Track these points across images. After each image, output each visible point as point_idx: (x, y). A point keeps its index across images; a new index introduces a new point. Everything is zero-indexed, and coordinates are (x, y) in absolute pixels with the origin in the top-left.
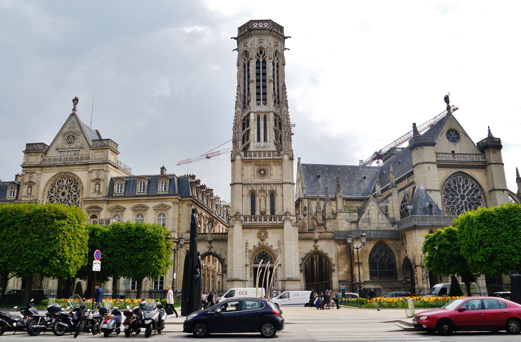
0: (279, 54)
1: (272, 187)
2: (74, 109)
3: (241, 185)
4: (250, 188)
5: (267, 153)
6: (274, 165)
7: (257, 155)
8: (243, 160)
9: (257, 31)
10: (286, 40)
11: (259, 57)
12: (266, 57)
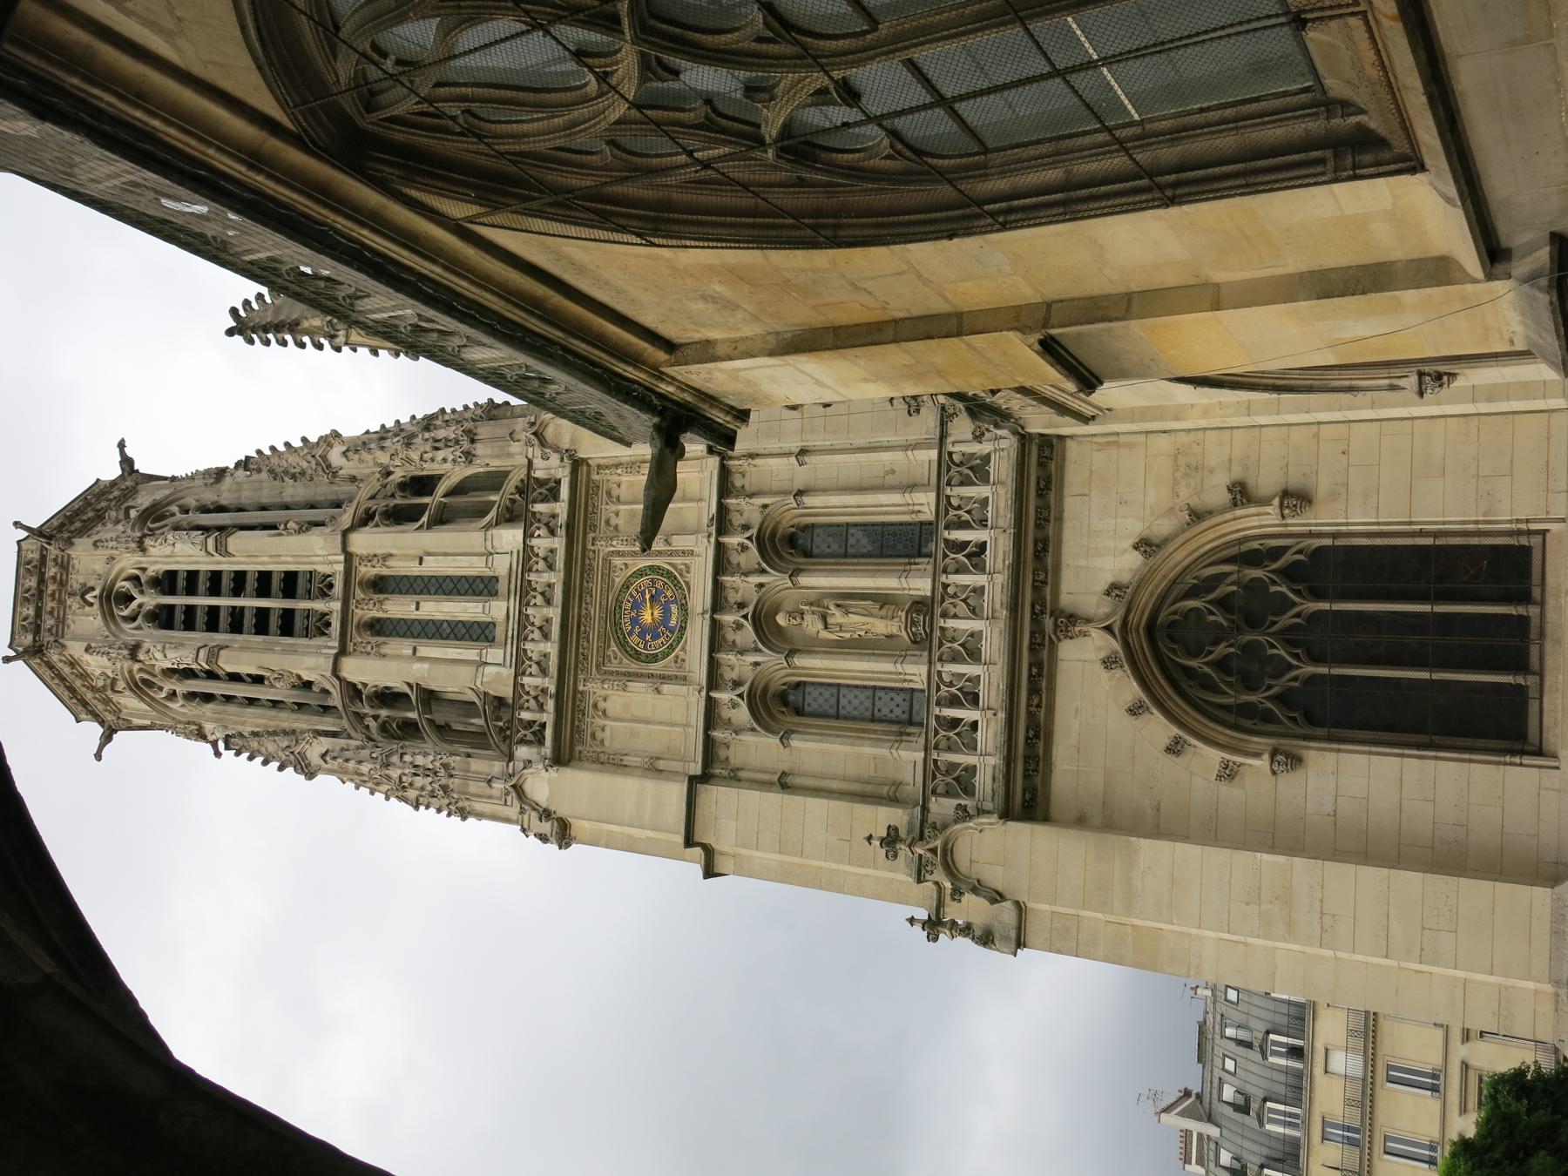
0: (169, 504)
4: (742, 714)
9: (45, 616)
10: (142, 466)
11: (140, 606)
12: (144, 570)
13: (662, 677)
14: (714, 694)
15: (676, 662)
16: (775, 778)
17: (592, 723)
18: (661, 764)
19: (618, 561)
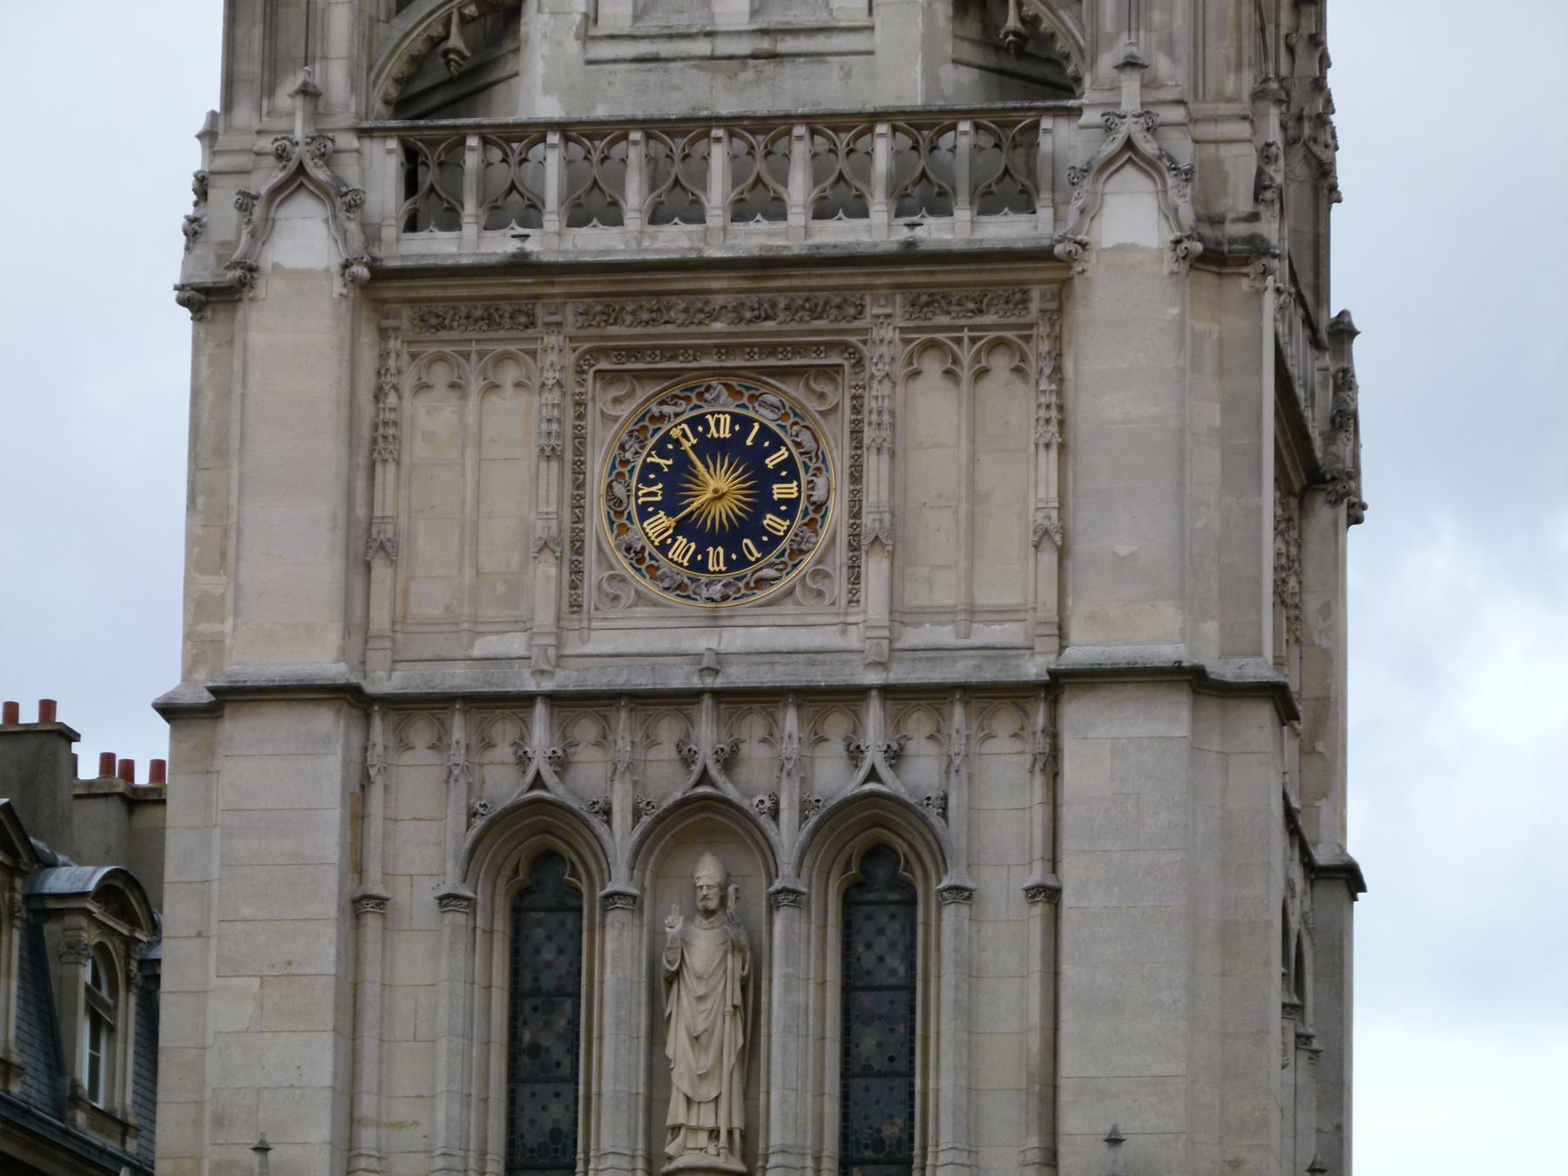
1: (874, 756)
3: (325, 721)
5: (800, 151)
6: (932, 367)
7: (635, 196)
8: (381, 274)
13: (579, 551)
14: (540, 710)
15: (612, 577)
16: (376, 889)
17: (466, 355)
18: (381, 570)
19: (839, 396)
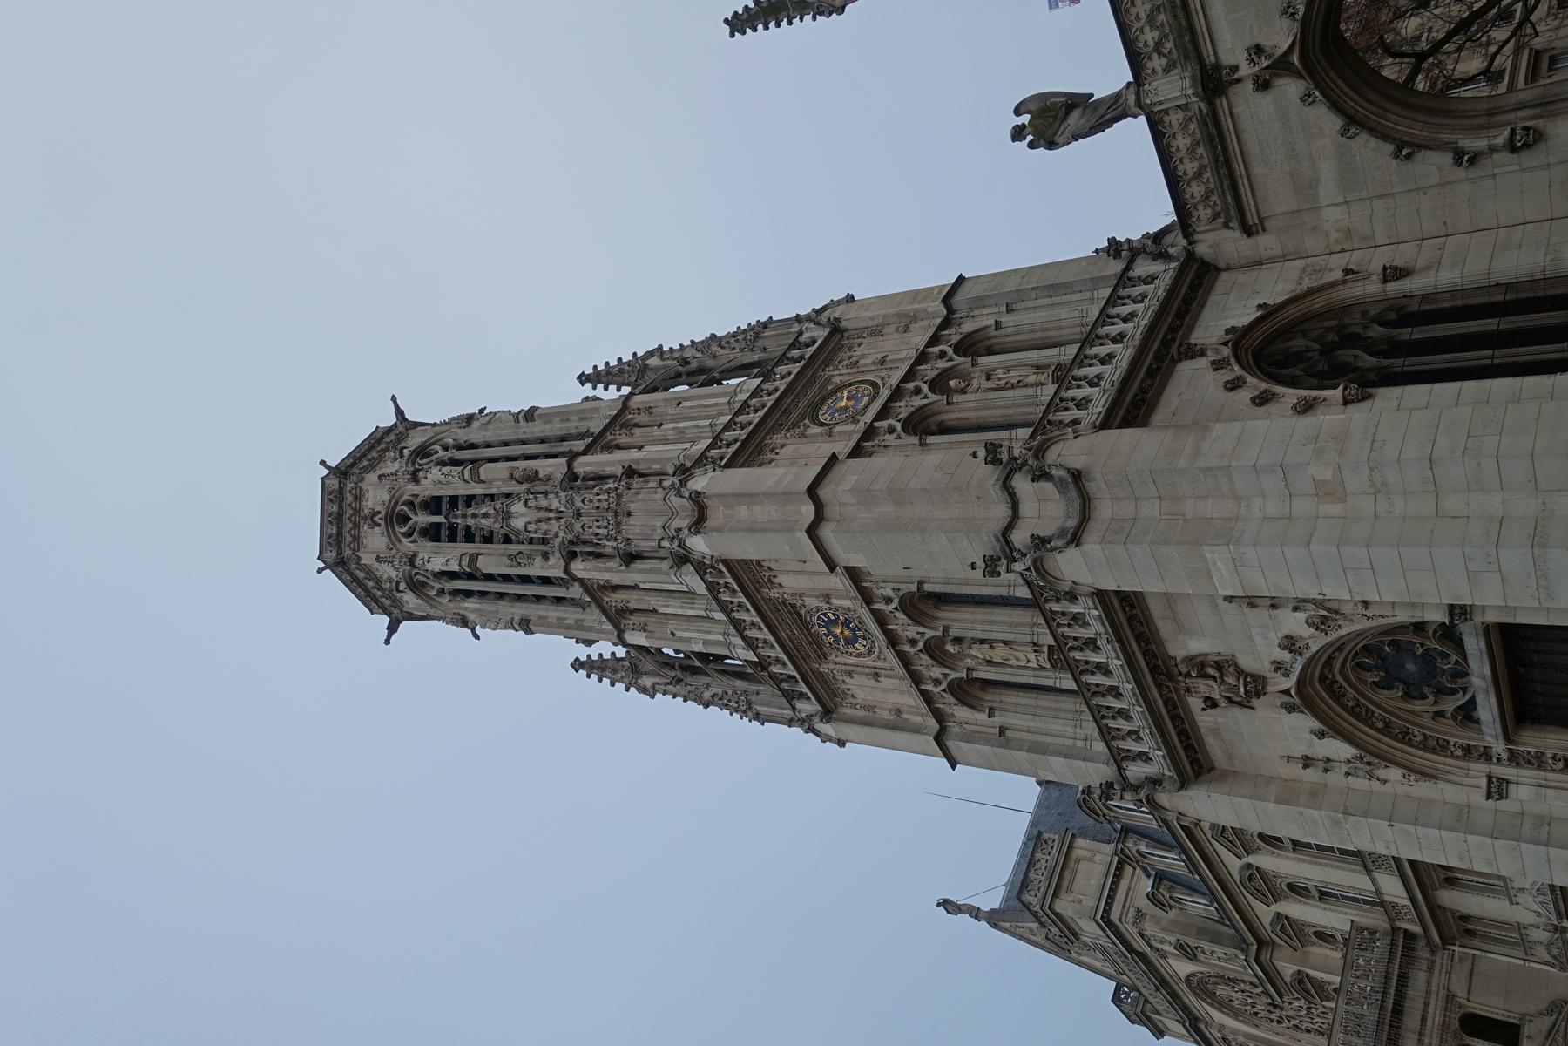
0: (396, 503)
2: (976, 913)
18: (905, 716)
